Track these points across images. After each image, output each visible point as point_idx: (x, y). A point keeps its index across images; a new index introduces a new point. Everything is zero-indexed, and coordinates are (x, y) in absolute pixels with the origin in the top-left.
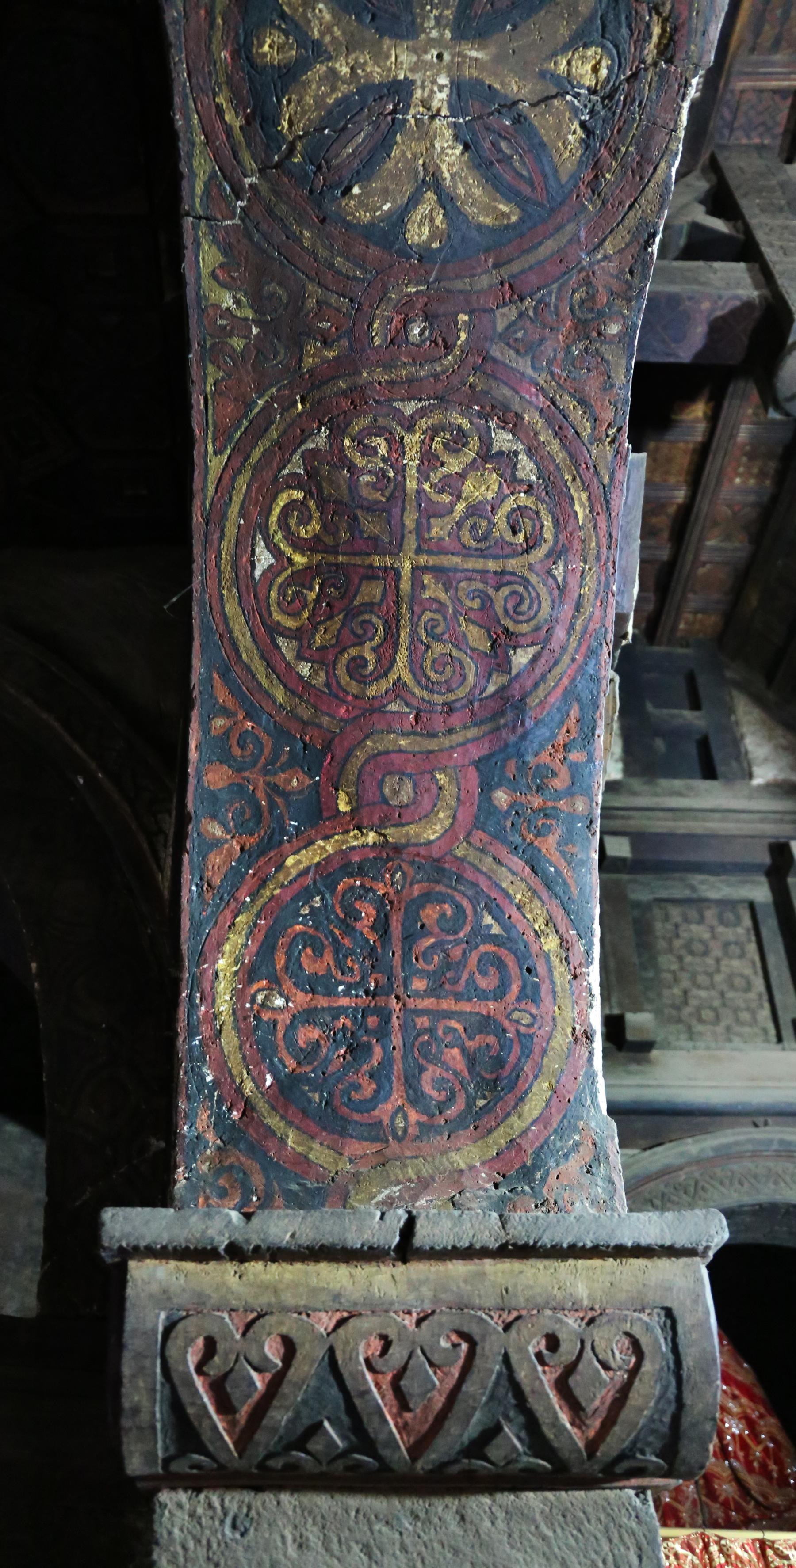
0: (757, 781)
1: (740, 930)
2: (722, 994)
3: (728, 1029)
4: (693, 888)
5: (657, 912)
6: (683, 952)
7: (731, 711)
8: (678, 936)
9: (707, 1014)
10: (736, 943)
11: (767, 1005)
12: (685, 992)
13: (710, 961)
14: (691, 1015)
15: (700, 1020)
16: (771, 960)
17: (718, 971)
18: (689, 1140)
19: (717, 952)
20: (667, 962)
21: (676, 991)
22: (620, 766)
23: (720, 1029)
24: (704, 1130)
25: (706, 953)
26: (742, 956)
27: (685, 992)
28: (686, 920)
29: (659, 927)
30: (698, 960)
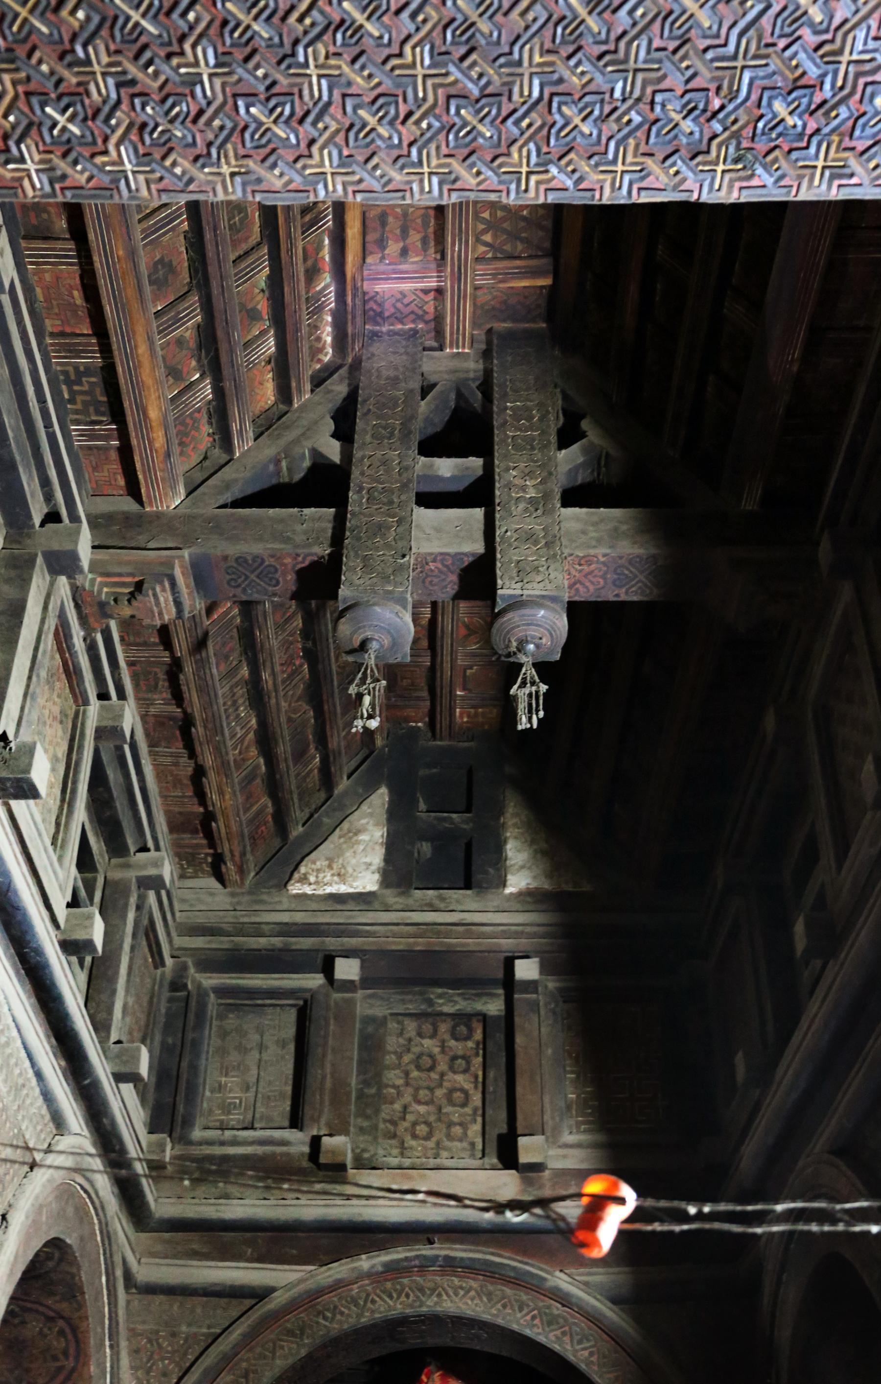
0: (509, 890)
1: (470, 1044)
2: (440, 1109)
3: (438, 1144)
4: (430, 1003)
5: (393, 1025)
6: (412, 1067)
7: (501, 812)
8: (409, 1051)
9: (422, 1129)
10: (463, 1057)
11: (479, 1119)
12: (405, 1107)
13: (434, 1076)
14: (406, 1130)
15: (415, 1136)
16: (491, 1074)
17: (440, 1085)
18: (364, 1257)
19: (442, 1066)
20: (393, 1077)
21: (397, 1106)
22: (377, 877)
23: (431, 1144)
24: (381, 1247)
25: (432, 1068)
26: (466, 1071)
27: (405, 1107)
28: (420, 1035)
29: (392, 1042)
30: (424, 1075)
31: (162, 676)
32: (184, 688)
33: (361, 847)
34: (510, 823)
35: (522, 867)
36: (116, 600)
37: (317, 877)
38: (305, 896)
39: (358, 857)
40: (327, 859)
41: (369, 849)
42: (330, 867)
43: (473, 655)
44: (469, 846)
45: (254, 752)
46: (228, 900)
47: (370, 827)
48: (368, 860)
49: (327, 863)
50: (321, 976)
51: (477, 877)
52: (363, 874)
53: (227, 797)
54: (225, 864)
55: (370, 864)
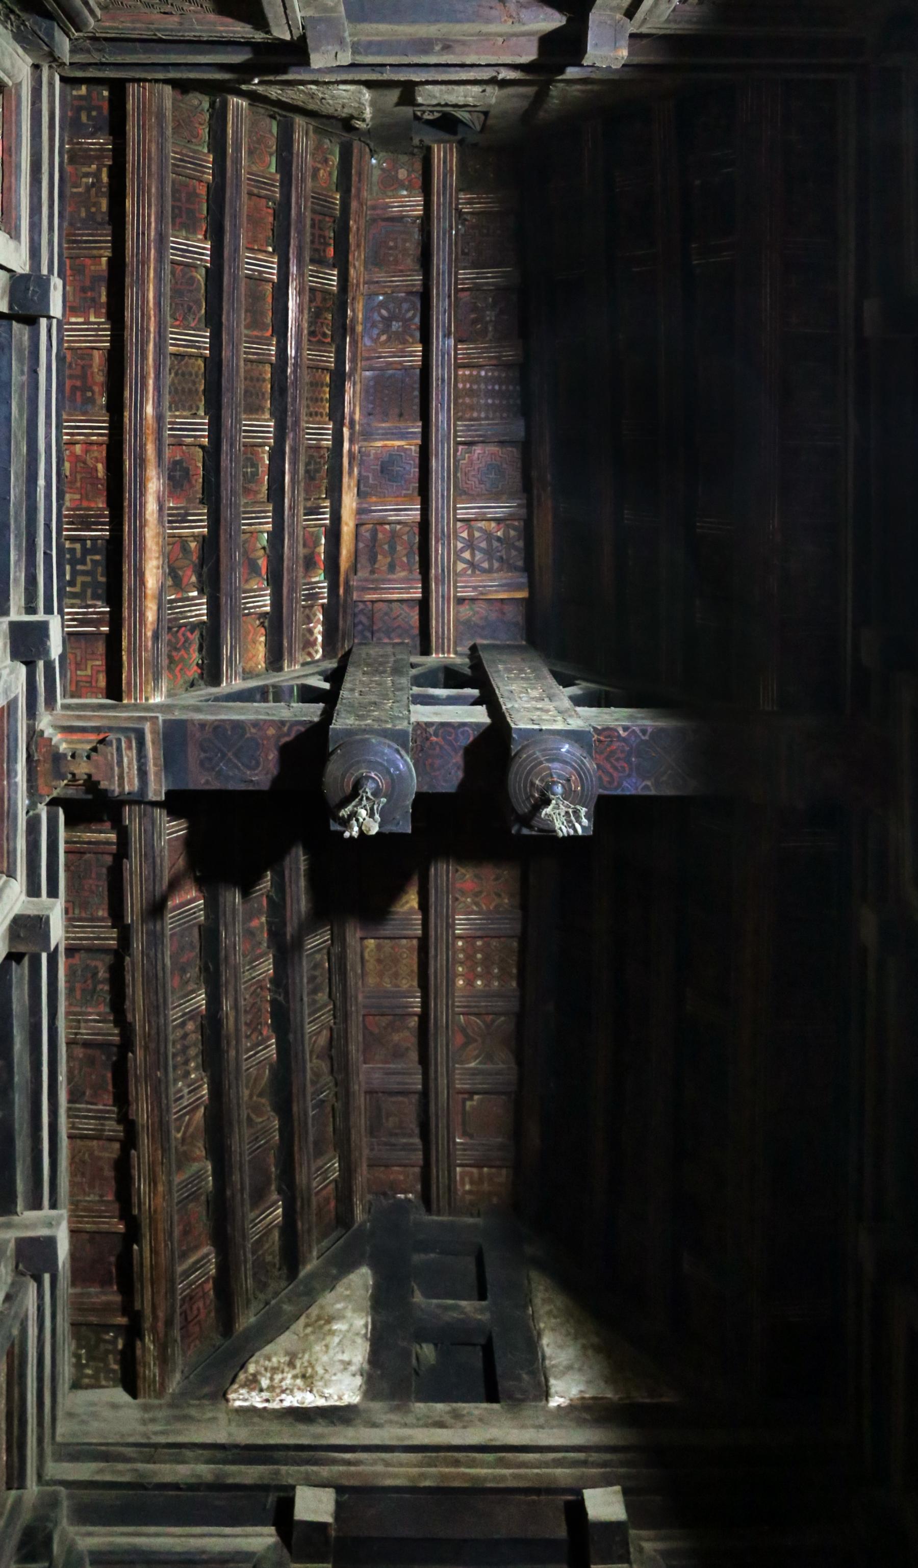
22: (358, 1381)
31: (102, 974)
32: (128, 978)
33: (336, 1340)
34: (542, 1312)
35: (569, 1368)
36: (73, 756)
37: (272, 1379)
38: (253, 1410)
39: (331, 1352)
40: (287, 1353)
41: (347, 1342)
42: (291, 1365)
43: (474, 1073)
44: (488, 1350)
45: (200, 1150)
46: (137, 1414)
47: (349, 1314)
48: (346, 1357)
49: (287, 1359)
50: (272, 1530)
51: (504, 1384)
52: (339, 1375)
53: (160, 1188)
54: (142, 1339)
55: (349, 1363)
